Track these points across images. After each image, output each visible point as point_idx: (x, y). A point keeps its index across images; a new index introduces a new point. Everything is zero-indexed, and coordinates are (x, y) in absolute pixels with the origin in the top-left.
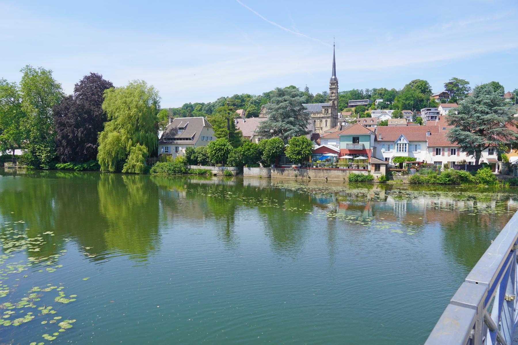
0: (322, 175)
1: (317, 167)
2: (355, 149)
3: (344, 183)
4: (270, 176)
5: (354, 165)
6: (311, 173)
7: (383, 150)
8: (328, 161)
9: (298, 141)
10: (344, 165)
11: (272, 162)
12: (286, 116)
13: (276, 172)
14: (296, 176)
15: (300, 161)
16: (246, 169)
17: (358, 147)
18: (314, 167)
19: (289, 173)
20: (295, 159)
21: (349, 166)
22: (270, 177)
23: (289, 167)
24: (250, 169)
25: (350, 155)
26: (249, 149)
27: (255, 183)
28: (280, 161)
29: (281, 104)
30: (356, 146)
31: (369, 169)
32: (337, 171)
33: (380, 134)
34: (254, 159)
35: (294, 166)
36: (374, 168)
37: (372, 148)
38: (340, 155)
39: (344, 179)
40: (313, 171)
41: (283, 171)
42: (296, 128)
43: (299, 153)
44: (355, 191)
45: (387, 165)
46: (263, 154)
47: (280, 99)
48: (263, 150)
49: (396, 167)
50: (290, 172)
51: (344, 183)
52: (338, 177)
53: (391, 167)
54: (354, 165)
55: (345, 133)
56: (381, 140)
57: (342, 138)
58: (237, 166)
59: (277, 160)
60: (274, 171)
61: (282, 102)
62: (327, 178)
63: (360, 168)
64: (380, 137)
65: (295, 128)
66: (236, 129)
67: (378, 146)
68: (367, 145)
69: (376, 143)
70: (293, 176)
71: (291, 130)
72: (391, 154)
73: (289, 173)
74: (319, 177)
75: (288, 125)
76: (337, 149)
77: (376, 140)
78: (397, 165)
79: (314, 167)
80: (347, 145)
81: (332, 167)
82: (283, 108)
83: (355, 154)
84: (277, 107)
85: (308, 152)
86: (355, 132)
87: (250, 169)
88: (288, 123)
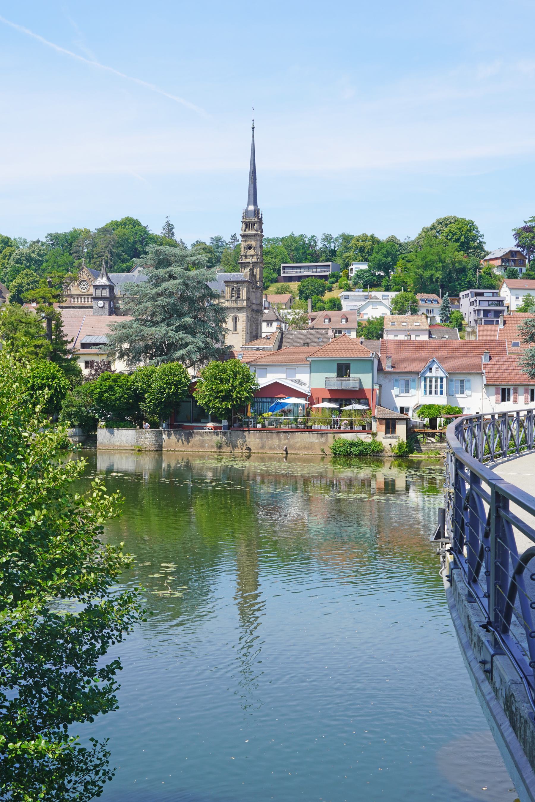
0: (277, 442)
1: (264, 426)
2: (344, 388)
3: (323, 458)
4: (161, 446)
5: (344, 422)
6: (252, 440)
7: (395, 391)
8: (284, 413)
9: (224, 371)
10: (323, 422)
11: (163, 416)
12: (171, 313)
13: (173, 437)
14: (220, 447)
15: (228, 414)
16: (102, 434)
17: (350, 383)
18: (259, 426)
19: (203, 441)
20: (219, 408)
21: (333, 424)
22: (159, 450)
23: (202, 428)
24: (112, 433)
25: (330, 401)
26: (111, 388)
27: (125, 464)
28: (177, 413)
29: (165, 285)
30: (344, 382)
31: (374, 429)
32: (306, 435)
33: (389, 358)
34: (125, 408)
35: (210, 425)
36: (383, 427)
37: (376, 387)
38: (311, 400)
39: (323, 451)
40: (257, 434)
41: (189, 435)
42: (199, 341)
43: (227, 397)
44: (347, 473)
45: (407, 420)
46: (143, 400)
47: (161, 272)
48: (145, 391)
49: (424, 426)
50: (206, 437)
51: (323, 458)
52: (310, 447)
53: (415, 426)
54: (344, 422)
55: (324, 354)
56: (391, 369)
57: (315, 365)
58: (80, 426)
59: (176, 410)
60: (169, 435)
61: (164, 280)
62: (286, 450)
63: (356, 428)
64: (389, 363)
65: (195, 340)
66: (67, 342)
67: (385, 382)
68: (367, 380)
69: (382, 376)
70: (212, 447)
71: (186, 345)
72: (412, 399)
73: (203, 441)
74: (271, 448)
76: (304, 389)
77: (380, 369)
78: (425, 422)
79: (259, 426)
80: (327, 379)
81: (297, 427)
82: (171, 294)
83: (342, 400)
84: (155, 290)
85: (246, 394)
86: (343, 355)
87: (112, 433)
88: (178, 329)
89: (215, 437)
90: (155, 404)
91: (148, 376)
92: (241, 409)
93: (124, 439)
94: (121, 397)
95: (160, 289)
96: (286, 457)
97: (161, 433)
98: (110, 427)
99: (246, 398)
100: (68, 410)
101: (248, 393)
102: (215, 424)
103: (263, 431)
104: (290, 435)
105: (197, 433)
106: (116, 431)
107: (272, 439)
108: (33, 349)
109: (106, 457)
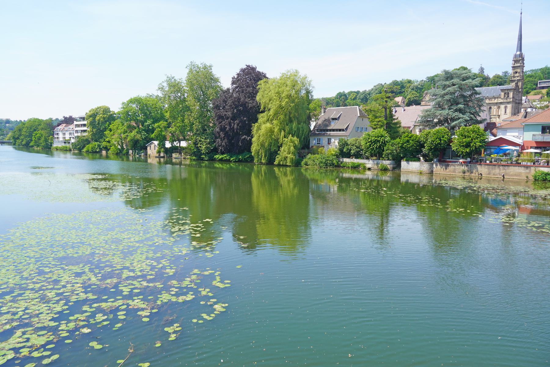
0: (498, 172)
1: (491, 162)
2: (545, 140)
3: (527, 182)
4: (432, 171)
5: (543, 160)
6: (482, 169)
8: (506, 155)
10: (529, 160)
11: (435, 156)
12: (454, 102)
13: (439, 167)
14: (464, 173)
15: (468, 155)
16: (404, 164)
18: (488, 162)
19: (455, 169)
22: (431, 172)
23: (455, 162)
24: (408, 163)
25: (536, 148)
26: (408, 141)
27: (414, 179)
28: (444, 154)
30: (545, 137)
34: (414, 151)
35: (461, 160)
38: (523, 148)
39: (527, 177)
41: (447, 166)
42: (466, 117)
43: (468, 145)
44: (543, 193)
46: (424, 147)
47: (447, 83)
50: (457, 167)
51: (527, 182)
52: (519, 174)
55: (530, 121)
57: (527, 127)
58: (393, 160)
59: (441, 153)
60: (437, 165)
61: (449, 86)
62: (503, 176)
65: (464, 116)
66: (395, 119)
70: (460, 172)
71: (459, 118)
73: (455, 169)
74: (494, 175)
75: (456, 114)
79: (488, 162)
80: (534, 135)
81: (512, 163)
82: (451, 94)
83: (544, 148)
84: (443, 92)
87: (408, 163)
88: (456, 110)
89: (461, 167)
90: (429, 149)
91: (426, 135)
92: (477, 151)
93: (414, 167)
94: (413, 145)
95: (446, 91)
96: (503, 180)
97: (433, 164)
98: (407, 161)
99: (480, 146)
100: (387, 152)
101: (480, 142)
102: (464, 160)
103: (490, 165)
104: (506, 168)
105: (452, 165)
106: (410, 163)
107: (495, 169)
108: (376, 123)
109: (405, 175)
